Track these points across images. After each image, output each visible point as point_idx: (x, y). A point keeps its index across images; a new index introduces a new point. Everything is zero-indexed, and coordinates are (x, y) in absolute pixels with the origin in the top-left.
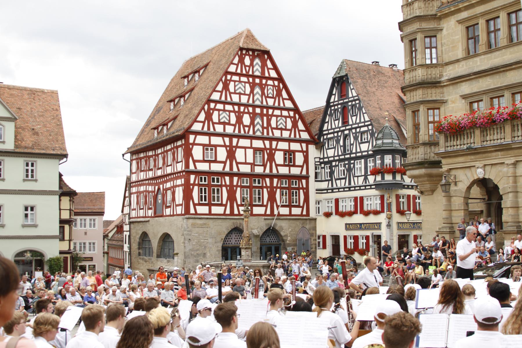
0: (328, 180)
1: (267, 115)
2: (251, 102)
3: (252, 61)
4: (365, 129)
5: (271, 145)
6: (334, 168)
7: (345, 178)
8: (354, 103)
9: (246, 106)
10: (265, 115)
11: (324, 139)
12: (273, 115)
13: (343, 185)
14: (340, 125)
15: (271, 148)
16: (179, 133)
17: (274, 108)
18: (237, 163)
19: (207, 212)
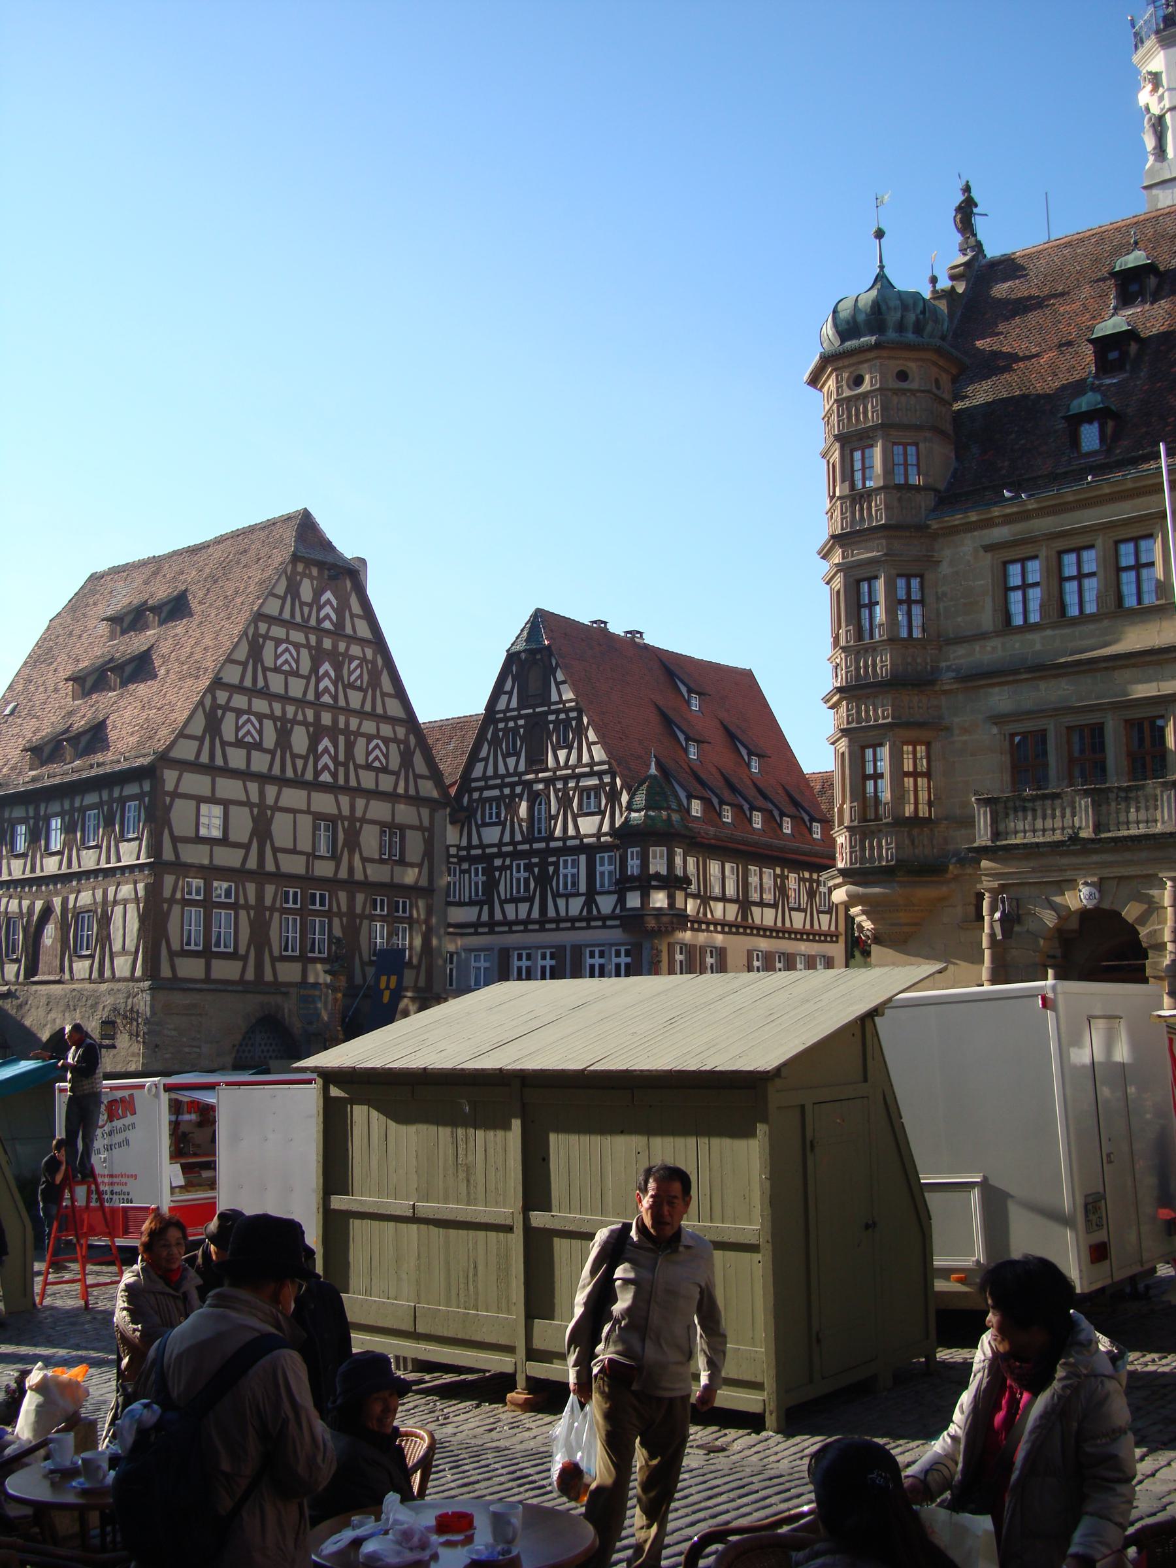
0: (480, 904)
1: (346, 732)
2: (311, 696)
3: (318, 594)
4: (594, 781)
5: (353, 808)
6: (497, 874)
7: (530, 900)
8: (562, 716)
9: (301, 703)
10: (342, 732)
11: (470, 800)
12: (358, 734)
13: (523, 915)
14: (522, 767)
15: (352, 818)
16: (145, 761)
17: (361, 714)
18: (275, 850)
19: (202, 975)
